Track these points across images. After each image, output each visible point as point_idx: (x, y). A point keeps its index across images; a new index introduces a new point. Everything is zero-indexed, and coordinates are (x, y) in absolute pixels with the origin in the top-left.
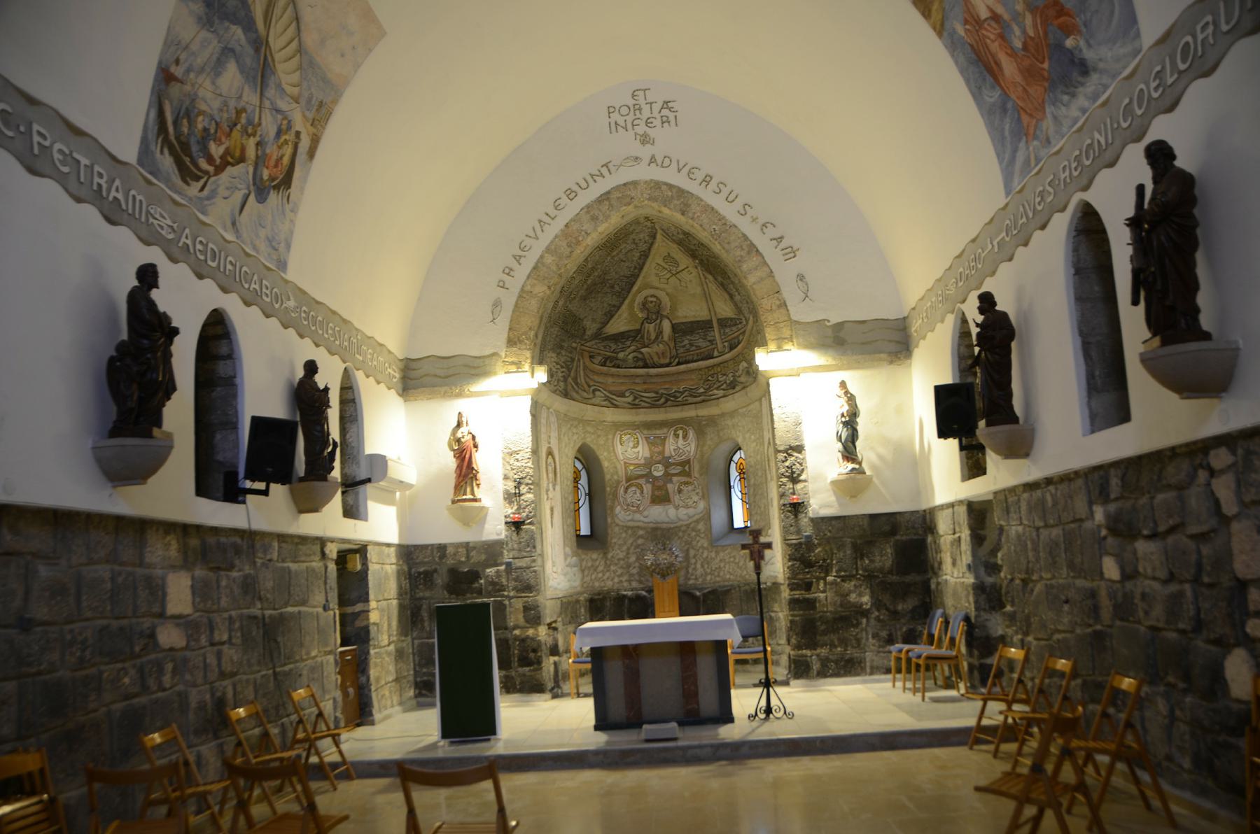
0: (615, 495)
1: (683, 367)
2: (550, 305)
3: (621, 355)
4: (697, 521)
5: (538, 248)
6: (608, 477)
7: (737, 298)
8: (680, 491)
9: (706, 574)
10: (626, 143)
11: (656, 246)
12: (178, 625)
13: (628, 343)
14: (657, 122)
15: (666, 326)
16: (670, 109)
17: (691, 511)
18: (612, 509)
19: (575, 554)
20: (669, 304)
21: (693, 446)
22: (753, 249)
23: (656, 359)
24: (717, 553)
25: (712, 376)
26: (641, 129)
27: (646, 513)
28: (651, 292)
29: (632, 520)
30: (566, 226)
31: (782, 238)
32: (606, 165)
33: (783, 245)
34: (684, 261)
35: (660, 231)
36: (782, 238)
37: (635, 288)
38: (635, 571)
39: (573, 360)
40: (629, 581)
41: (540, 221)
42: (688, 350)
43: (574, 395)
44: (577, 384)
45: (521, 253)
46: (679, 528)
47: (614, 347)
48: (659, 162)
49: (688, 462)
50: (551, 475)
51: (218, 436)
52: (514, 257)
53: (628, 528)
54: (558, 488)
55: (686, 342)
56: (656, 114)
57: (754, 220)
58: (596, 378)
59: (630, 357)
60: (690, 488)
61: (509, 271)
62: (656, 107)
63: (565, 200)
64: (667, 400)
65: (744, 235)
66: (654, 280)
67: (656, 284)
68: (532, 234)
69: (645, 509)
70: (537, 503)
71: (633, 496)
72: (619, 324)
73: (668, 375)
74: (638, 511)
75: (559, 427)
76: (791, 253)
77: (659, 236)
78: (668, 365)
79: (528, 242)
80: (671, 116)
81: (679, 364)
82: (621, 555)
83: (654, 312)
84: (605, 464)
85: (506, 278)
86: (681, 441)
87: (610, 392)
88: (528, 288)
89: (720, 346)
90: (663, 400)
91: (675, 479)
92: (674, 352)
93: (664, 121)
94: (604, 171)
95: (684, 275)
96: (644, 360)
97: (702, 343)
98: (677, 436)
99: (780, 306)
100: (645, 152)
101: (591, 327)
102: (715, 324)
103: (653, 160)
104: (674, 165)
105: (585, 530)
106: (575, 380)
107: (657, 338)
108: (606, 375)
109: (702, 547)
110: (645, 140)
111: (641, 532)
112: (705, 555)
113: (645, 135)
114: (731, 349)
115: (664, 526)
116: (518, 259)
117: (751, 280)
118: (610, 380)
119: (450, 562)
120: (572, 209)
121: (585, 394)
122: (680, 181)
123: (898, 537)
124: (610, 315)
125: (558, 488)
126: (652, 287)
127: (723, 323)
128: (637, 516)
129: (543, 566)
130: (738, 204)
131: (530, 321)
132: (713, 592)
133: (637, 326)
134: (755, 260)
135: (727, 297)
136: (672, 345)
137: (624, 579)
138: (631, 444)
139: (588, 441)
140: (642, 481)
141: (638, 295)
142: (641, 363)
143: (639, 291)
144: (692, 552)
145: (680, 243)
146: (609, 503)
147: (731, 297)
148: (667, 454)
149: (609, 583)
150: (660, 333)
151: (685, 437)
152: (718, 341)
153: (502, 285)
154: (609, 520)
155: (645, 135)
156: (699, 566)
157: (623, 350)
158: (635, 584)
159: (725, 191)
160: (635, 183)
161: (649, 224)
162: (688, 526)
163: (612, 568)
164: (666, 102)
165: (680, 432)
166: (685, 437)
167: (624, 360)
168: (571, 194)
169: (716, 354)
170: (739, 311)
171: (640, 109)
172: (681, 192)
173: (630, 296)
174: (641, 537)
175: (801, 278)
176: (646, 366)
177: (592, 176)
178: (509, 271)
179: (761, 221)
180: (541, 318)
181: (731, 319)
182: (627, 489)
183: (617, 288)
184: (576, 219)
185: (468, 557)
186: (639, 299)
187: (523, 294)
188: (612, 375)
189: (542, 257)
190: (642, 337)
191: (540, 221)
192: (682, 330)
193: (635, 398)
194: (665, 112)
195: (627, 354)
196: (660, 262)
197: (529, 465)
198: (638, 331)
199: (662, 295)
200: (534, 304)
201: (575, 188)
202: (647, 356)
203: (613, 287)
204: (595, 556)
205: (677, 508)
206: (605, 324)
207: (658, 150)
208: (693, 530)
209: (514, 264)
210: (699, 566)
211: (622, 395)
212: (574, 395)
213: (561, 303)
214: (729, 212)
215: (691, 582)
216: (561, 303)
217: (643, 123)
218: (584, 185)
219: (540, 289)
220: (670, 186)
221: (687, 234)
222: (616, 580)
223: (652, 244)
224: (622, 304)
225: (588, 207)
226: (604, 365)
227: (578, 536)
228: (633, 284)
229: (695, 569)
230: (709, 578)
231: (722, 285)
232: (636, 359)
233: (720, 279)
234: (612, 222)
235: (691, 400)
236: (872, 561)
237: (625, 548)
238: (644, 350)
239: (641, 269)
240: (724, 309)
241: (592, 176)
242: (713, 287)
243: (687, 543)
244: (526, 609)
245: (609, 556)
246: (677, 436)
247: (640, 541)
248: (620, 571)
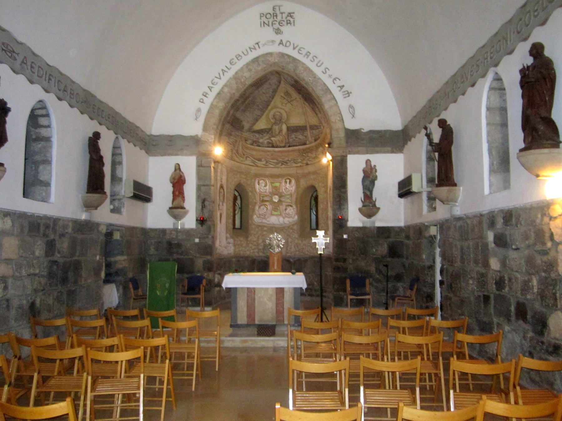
0: (254, 210)
1: (291, 148)
2: (225, 113)
3: (261, 141)
4: (293, 225)
5: (221, 83)
6: (251, 200)
7: (320, 115)
8: (286, 209)
10: (268, 33)
11: (281, 86)
12: (8, 264)
13: (265, 135)
14: (285, 23)
15: (284, 127)
16: (291, 16)
17: (291, 220)
18: (252, 216)
19: (232, 237)
20: (286, 116)
21: (294, 188)
22: (328, 91)
23: (278, 144)
25: (305, 153)
26: (276, 26)
27: (268, 219)
28: (278, 110)
29: (261, 222)
30: (236, 73)
31: (343, 86)
32: (257, 43)
33: (344, 89)
34: (294, 94)
35: (283, 79)
36: (343, 86)
37: (270, 108)
38: (261, 247)
39: (236, 141)
40: (258, 252)
41: (222, 70)
42: (294, 140)
43: (236, 159)
44: (238, 153)
45: (211, 85)
46: (284, 227)
47: (257, 135)
48: (284, 44)
49: (291, 195)
50: (221, 198)
51: (41, 167)
52: (209, 87)
53: (259, 226)
54: (225, 204)
55: (293, 136)
56: (284, 19)
57: (330, 76)
58: (248, 151)
59: (266, 142)
60: (291, 208)
61: (205, 95)
62: (285, 16)
63: (236, 60)
64: (282, 164)
65: (324, 84)
66: (279, 105)
67: (280, 105)
68: (218, 76)
69: (268, 217)
70: (212, 213)
71: (263, 210)
72: (261, 125)
73: (283, 152)
74: (265, 218)
75: (228, 174)
76: (348, 94)
77: (282, 82)
78: (284, 147)
79: (216, 80)
80: (292, 20)
81: (289, 146)
82: (255, 239)
83: (278, 121)
84: (250, 194)
85: (203, 97)
86: (288, 185)
87: (254, 158)
88: (215, 103)
89: (310, 139)
90: (280, 164)
92: (287, 140)
93: (289, 23)
94: (257, 46)
95: (294, 103)
96: (272, 144)
97: (301, 137)
98: (286, 182)
99: (339, 121)
100: (278, 38)
101: (246, 126)
102: (308, 128)
103: (281, 43)
104: (292, 47)
105: (238, 224)
106: (237, 151)
107: (279, 133)
108: (253, 149)
109: (295, 238)
110: (278, 32)
111: (265, 229)
113: (278, 29)
114: (316, 140)
115: (277, 226)
116: (210, 88)
117: (326, 106)
118: (254, 153)
119: (167, 237)
120: (240, 64)
121: (241, 159)
122: (294, 54)
123: (391, 240)
124: (257, 120)
125: (225, 204)
126: (278, 108)
127: (312, 127)
128: (264, 221)
129: (214, 242)
130: (322, 68)
131: (214, 120)
132: (299, 260)
133: (270, 127)
134: (329, 96)
135: (315, 115)
136: (286, 137)
137: (256, 251)
138: (263, 185)
139: (242, 182)
140: (267, 203)
141: (271, 112)
142: (270, 145)
143: (272, 109)
144: (290, 240)
145: (292, 86)
146: (251, 213)
147: (317, 114)
148: (281, 191)
149: (248, 253)
150: (281, 131)
151: (290, 182)
152: (309, 135)
153: (202, 101)
154: (250, 222)
155: (278, 29)
156: (293, 247)
157: (262, 138)
158: (261, 254)
159: (317, 60)
160: (271, 54)
161: (277, 75)
162: (289, 227)
163: (250, 245)
164: (290, 13)
165: (288, 181)
166: (290, 182)
167: (262, 143)
168: (238, 57)
169: (308, 142)
170: (321, 123)
171: (276, 16)
172: (294, 60)
173: (267, 111)
174: (266, 231)
175: (351, 107)
176: (273, 147)
177: (250, 48)
178: (205, 95)
179: (334, 77)
180: (220, 119)
181: (316, 126)
182: (260, 207)
183: (261, 107)
184: (241, 70)
185: (177, 236)
186: (272, 113)
187: (212, 107)
188: (256, 150)
189: (222, 88)
190: (272, 132)
191: (222, 70)
192: (292, 130)
193: (267, 162)
194: (289, 18)
195: (264, 140)
196: (282, 94)
198: (270, 129)
199: (282, 111)
200: (217, 112)
201: (241, 54)
202: (274, 141)
203: (258, 106)
204: (242, 239)
205: (284, 218)
206: (254, 124)
207: (285, 37)
208: (292, 229)
209: (208, 90)
211: (260, 160)
212: (236, 159)
213: (231, 113)
214: (318, 71)
215: (288, 254)
216: (231, 113)
217: (277, 23)
218: (246, 53)
219: (221, 105)
220: (289, 56)
221: (296, 81)
222: (252, 251)
223: (279, 86)
224: (262, 115)
225: (248, 65)
226: (252, 144)
227: (234, 228)
228: (268, 105)
229: (291, 248)
230: (297, 253)
231: (313, 108)
232: (269, 143)
233: (311, 105)
234: (258, 71)
235: (294, 165)
236: (376, 250)
237: (257, 236)
238: (273, 139)
239: (273, 98)
240: (314, 121)
241: (250, 48)
242: (308, 110)
244: (205, 263)
245: (249, 239)
246: (286, 182)
247: (265, 233)
248: (253, 247)
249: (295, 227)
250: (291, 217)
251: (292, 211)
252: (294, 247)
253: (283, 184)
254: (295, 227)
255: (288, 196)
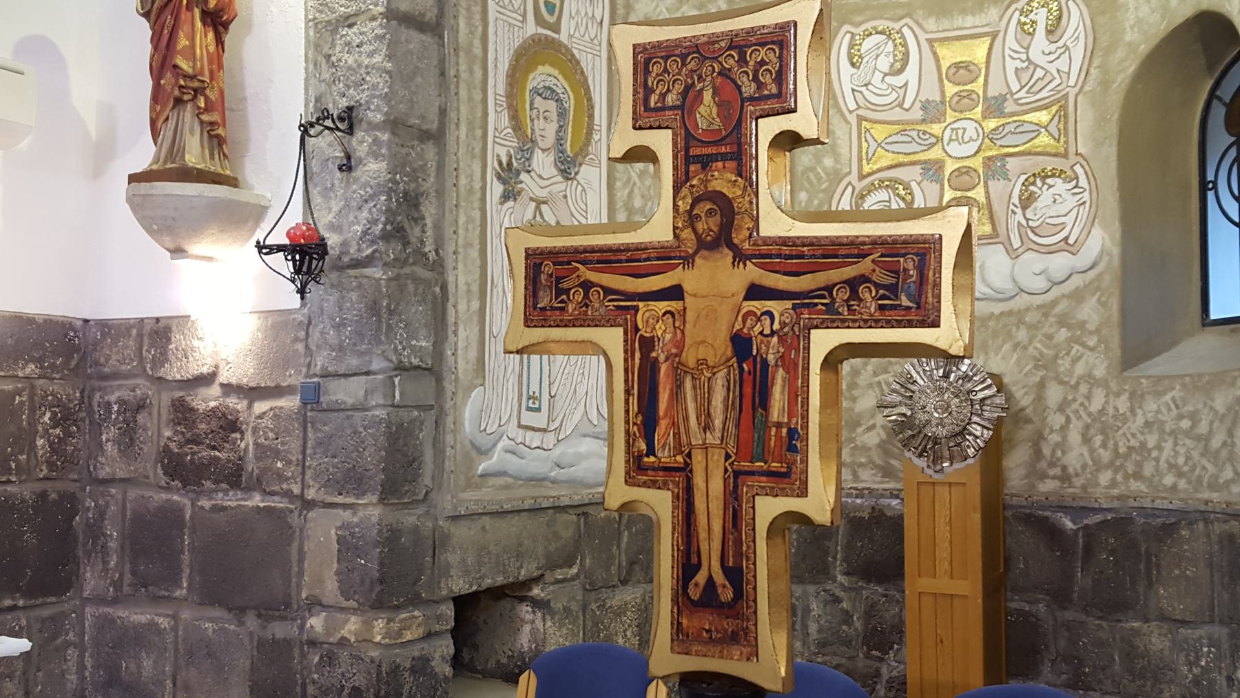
4: (1077, 296)
8: (1027, 201)
9: (1099, 466)
17: (1060, 263)
24: (1136, 398)
60: (1059, 186)
91: (1012, 163)
98: (1026, 30)
109: (1089, 377)
112: (1095, 406)
132: (1120, 524)
156: (1074, 437)
162: (1045, 310)
197: (378, 59)
208: (1063, 322)
210: (1074, 437)
230: (1105, 478)
243: (1040, 363)
246: (1026, 30)
249: (1089, 312)
250: (1067, 246)
251: (1060, 203)
252: (1086, 440)
253: (1011, 42)
254: (1089, 312)
255: (1043, 117)
